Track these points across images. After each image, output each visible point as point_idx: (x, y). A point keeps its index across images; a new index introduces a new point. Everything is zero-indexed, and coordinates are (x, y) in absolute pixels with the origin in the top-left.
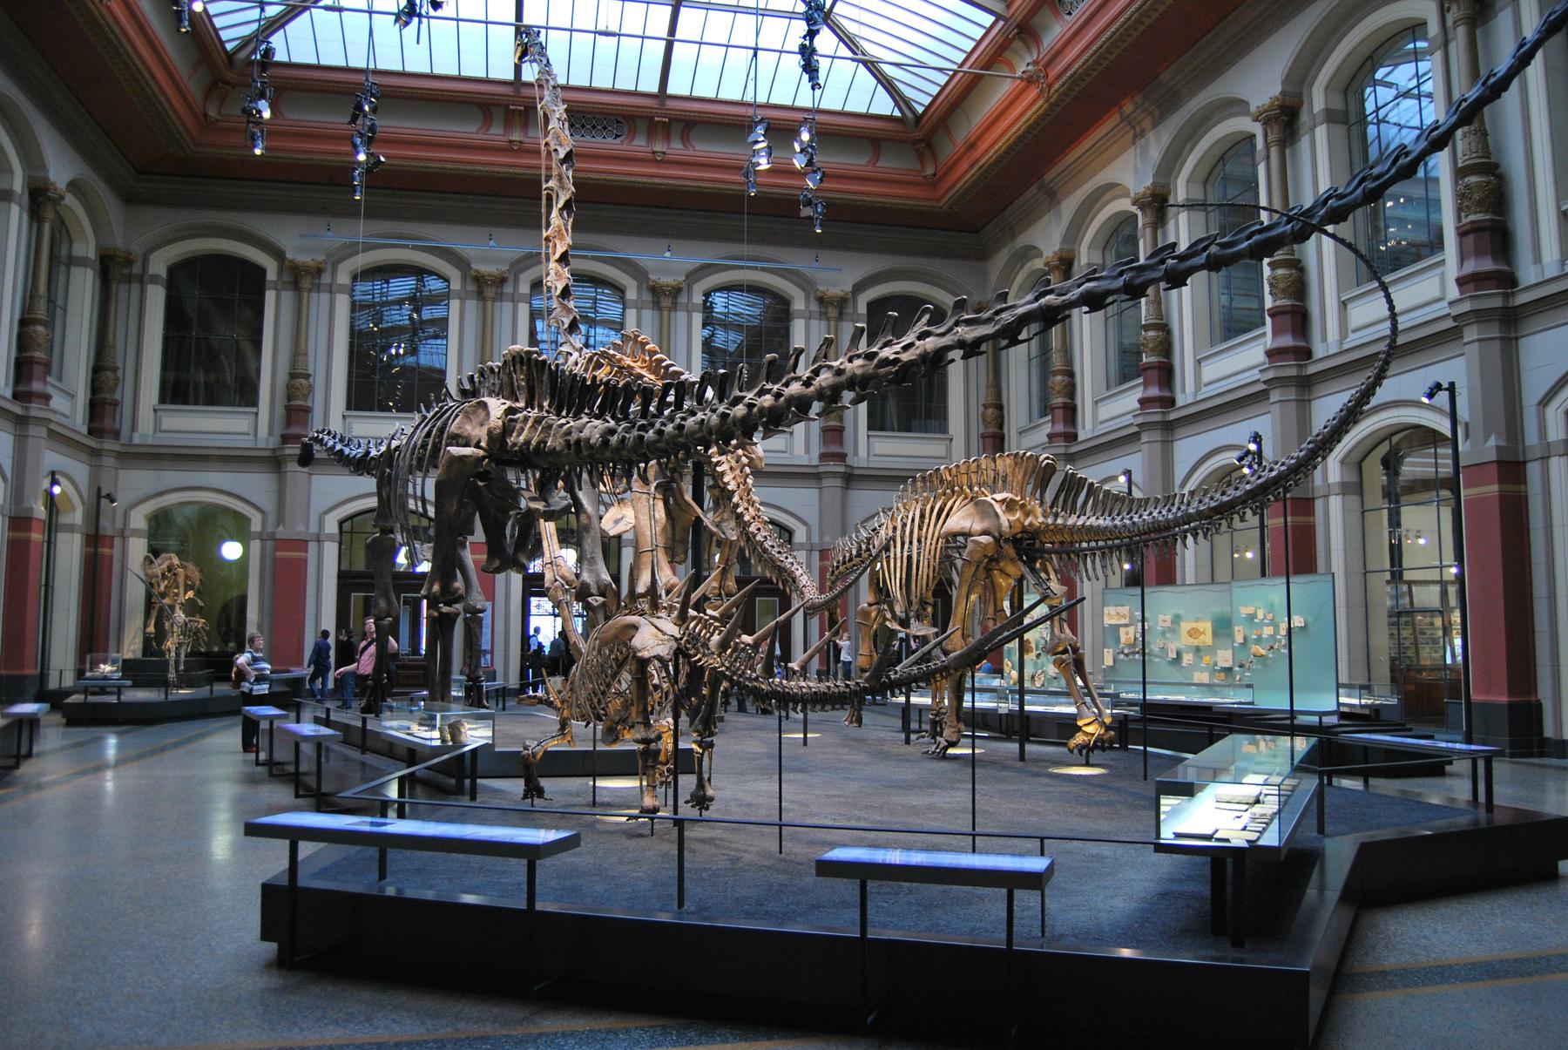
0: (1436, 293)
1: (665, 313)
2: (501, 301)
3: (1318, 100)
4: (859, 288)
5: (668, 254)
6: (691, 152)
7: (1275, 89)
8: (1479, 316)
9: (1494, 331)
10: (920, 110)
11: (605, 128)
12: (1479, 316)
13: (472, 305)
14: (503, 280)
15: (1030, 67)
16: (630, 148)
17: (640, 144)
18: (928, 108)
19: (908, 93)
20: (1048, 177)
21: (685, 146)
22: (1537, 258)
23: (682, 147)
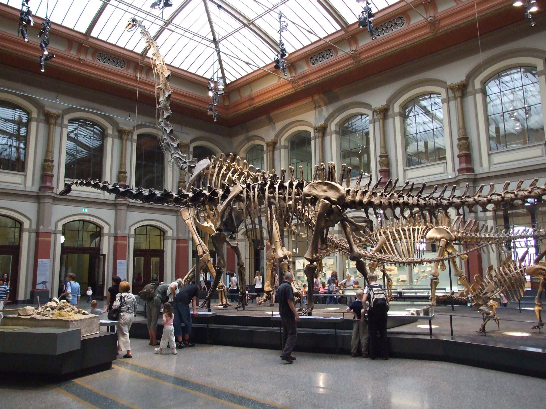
0: (442, 171)
1: (124, 141)
2: (55, 126)
3: (396, 108)
4: (192, 141)
5: (129, 118)
6: (149, 80)
7: (384, 103)
8: (468, 180)
9: (471, 184)
10: (228, 82)
11: (118, 63)
12: (468, 180)
13: (42, 126)
14: (57, 117)
15: (292, 78)
16: (126, 73)
17: (130, 72)
18: (232, 83)
19: (226, 74)
20: (272, 114)
21: (147, 76)
22: (481, 165)
23: (145, 77)
